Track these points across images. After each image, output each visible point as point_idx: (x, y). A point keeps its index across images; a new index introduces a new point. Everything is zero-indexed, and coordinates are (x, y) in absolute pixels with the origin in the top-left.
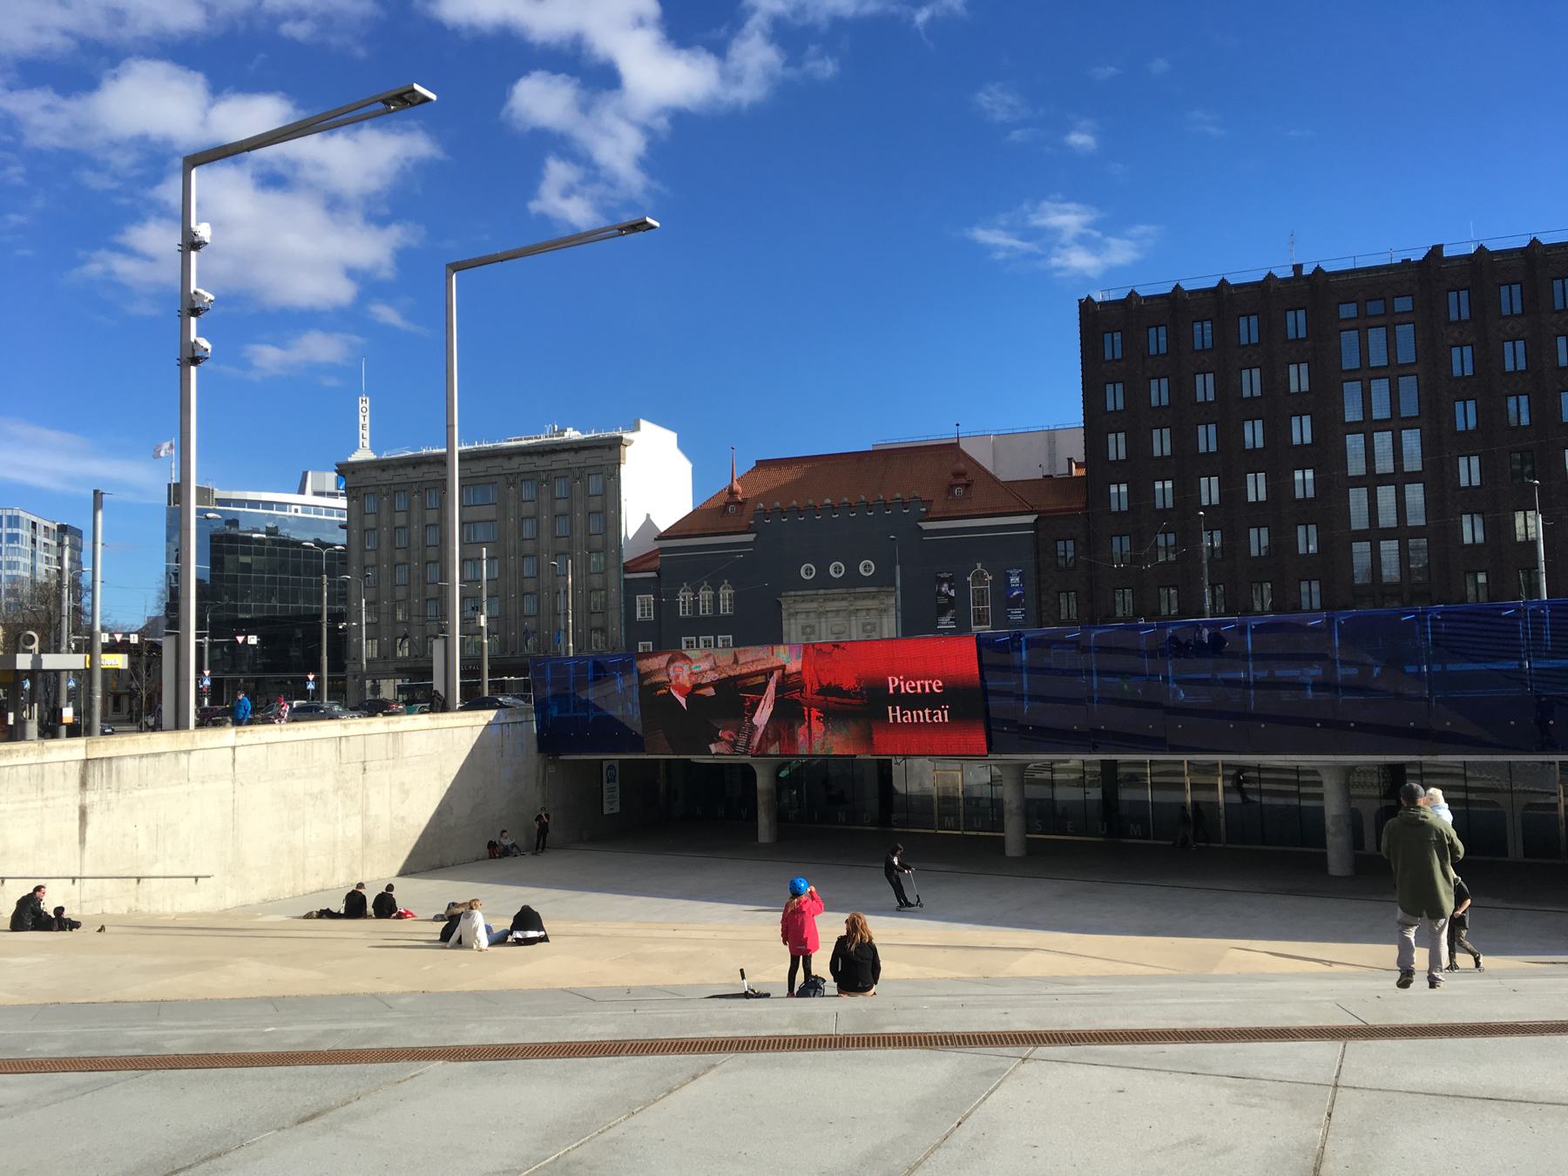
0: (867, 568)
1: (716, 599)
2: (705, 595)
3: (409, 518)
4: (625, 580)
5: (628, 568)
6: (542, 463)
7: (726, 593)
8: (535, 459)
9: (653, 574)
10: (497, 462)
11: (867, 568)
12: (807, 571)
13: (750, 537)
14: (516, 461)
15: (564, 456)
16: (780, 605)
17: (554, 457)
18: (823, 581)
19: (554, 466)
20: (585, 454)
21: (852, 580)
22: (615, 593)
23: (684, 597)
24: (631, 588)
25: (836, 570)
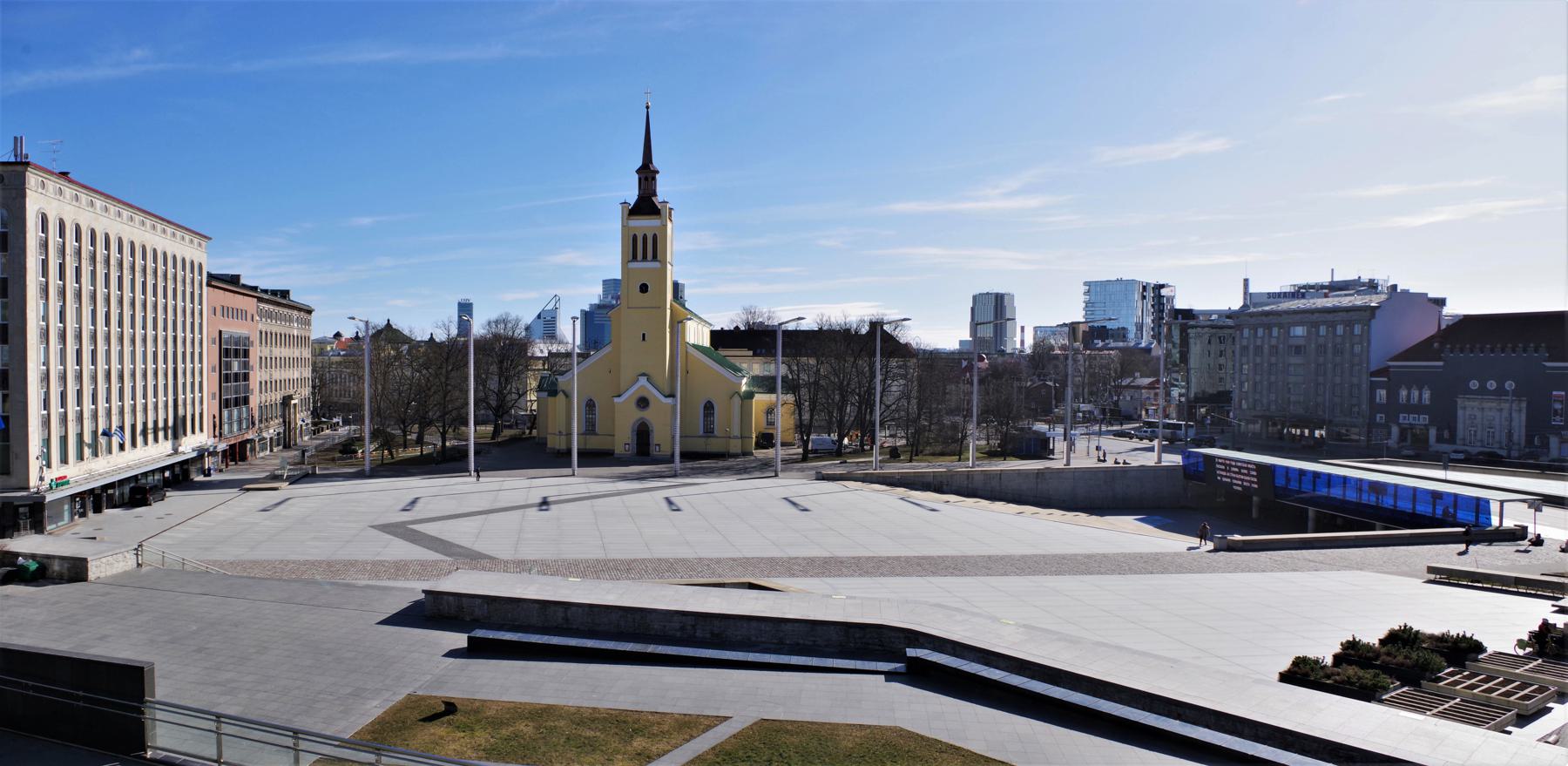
0: (1510, 385)
1: (1420, 395)
2: (1416, 393)
3: (1263, 342)
4: (1371, 381)
5: (1373, 374)
6: (1330, 317)
7: (1427, 395)
8: (1326, 315)
9: (1386, 379)
10: (1307, 315)
11: (1510, 385)
12: (1474, 384)
13: (1441, 363)
14: (1317, 315)
15: (1340, 314)
16: (1456, 402)
17: (1336, 314)
18: (1483, 391)
19: (1336, 319)
20: (1352, 313)
21: (1500, 392)
22: (1365, 386)
23: (1404, 393)
24: (1373, 387)
25: (1492, 385)
